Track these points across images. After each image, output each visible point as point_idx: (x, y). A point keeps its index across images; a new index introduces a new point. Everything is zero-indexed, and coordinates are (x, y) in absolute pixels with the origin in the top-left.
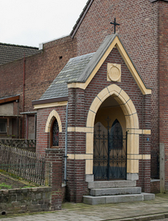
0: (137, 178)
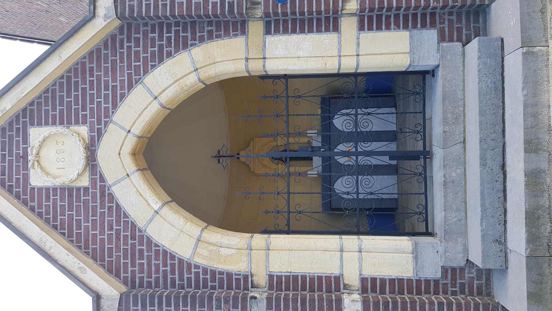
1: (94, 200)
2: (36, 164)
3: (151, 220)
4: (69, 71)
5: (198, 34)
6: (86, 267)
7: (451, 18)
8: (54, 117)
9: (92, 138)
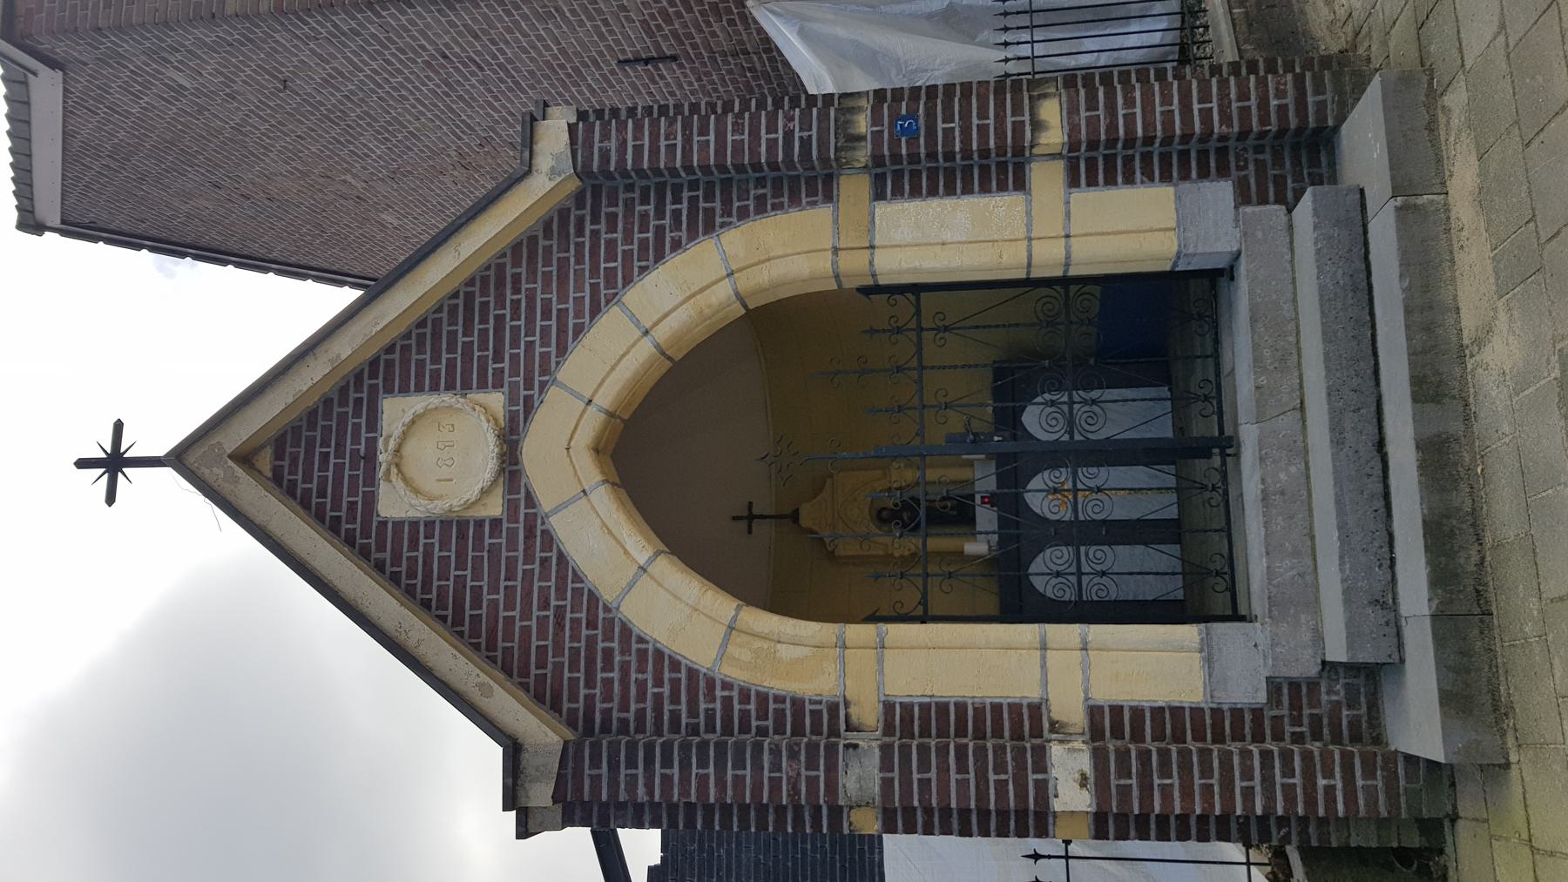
0: (1221, 192)
1: (512, 545)
2: (394, 470)
3: (631, 586)
4: (470, 282)
5: (736, 204)
6: (492, 683)
7: (1261, 157)
8: (435, 375)
9: (512, 418)
